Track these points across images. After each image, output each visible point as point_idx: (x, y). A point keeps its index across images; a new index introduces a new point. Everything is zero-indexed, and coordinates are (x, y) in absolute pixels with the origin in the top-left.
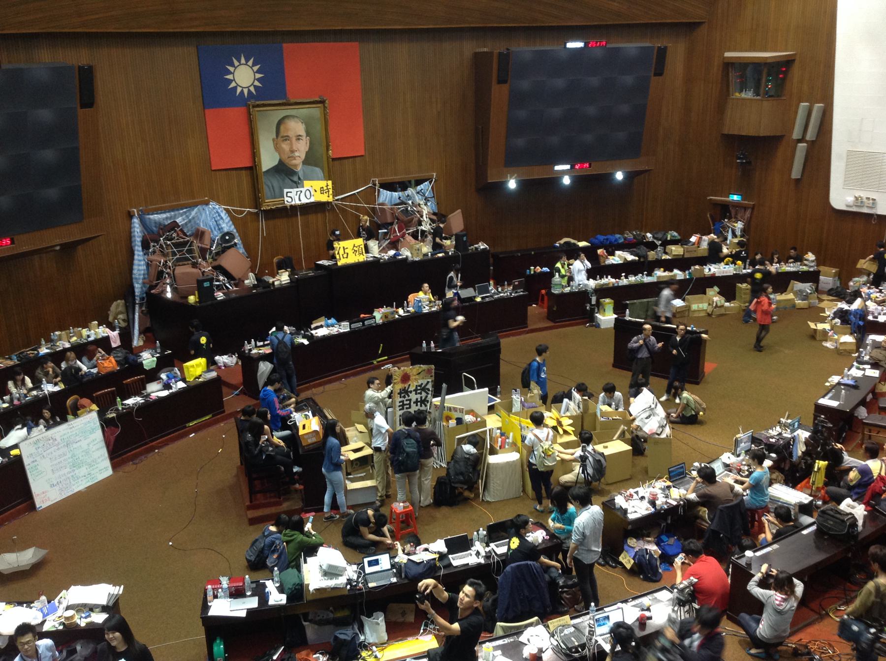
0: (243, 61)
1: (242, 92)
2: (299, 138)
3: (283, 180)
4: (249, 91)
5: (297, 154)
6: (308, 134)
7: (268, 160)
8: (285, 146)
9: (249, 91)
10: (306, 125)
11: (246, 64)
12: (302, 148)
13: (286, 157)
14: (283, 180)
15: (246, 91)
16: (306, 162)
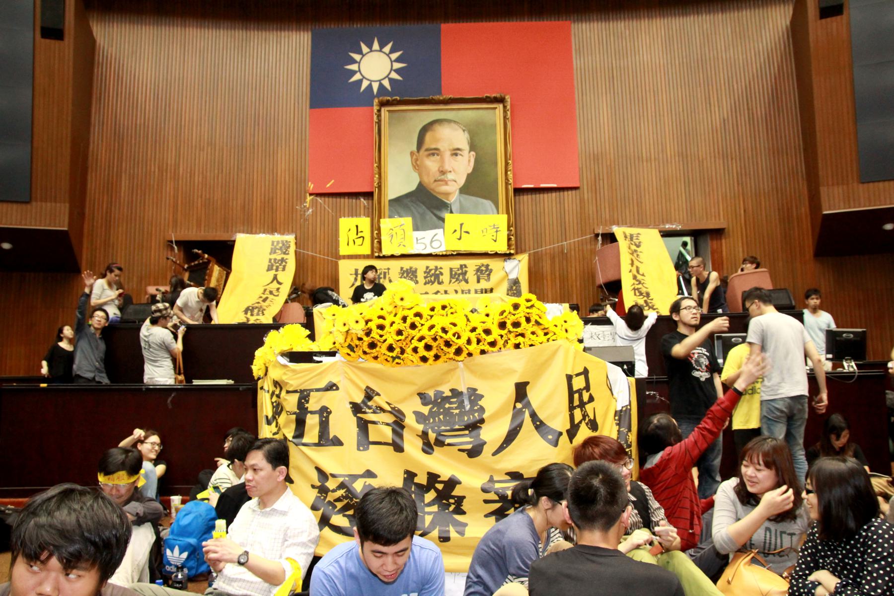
0: (376, 46)
1: (370, 87)
2: (456, 152)
3: (423, 216)
4: (381, 86)
5: (450, 176)
6: (472, 147)
7: (399, 180)
8: (432, 164)
9: (381, 86)
10: (470, 132)
11: (380, 51)
12: (461, 168)
13: (432, 181)
14: (423, 216)
15: (375, 87)
16: (464, 190)
